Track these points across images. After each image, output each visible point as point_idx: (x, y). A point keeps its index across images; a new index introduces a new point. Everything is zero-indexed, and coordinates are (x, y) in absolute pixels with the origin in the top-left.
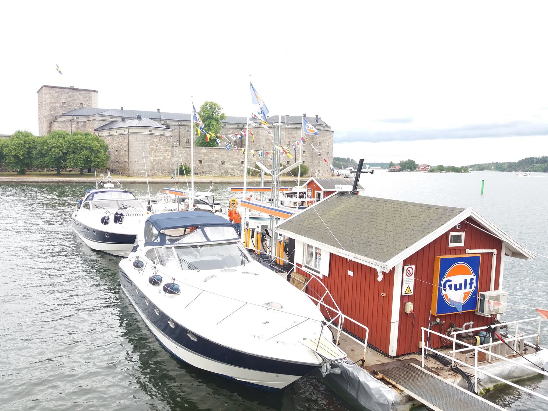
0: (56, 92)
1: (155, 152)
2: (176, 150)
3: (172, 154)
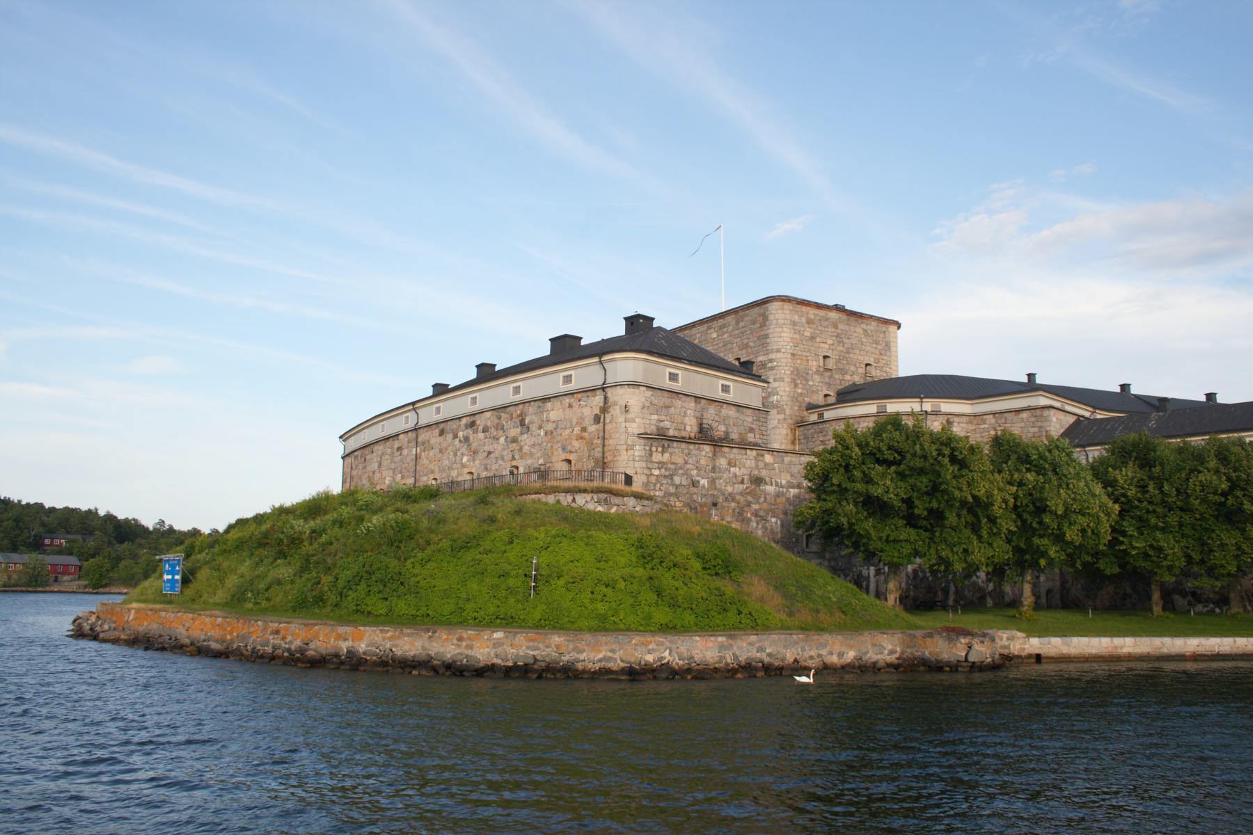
0: (809, 322)
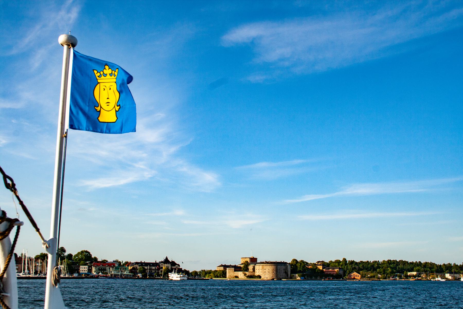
2: (235, 272)
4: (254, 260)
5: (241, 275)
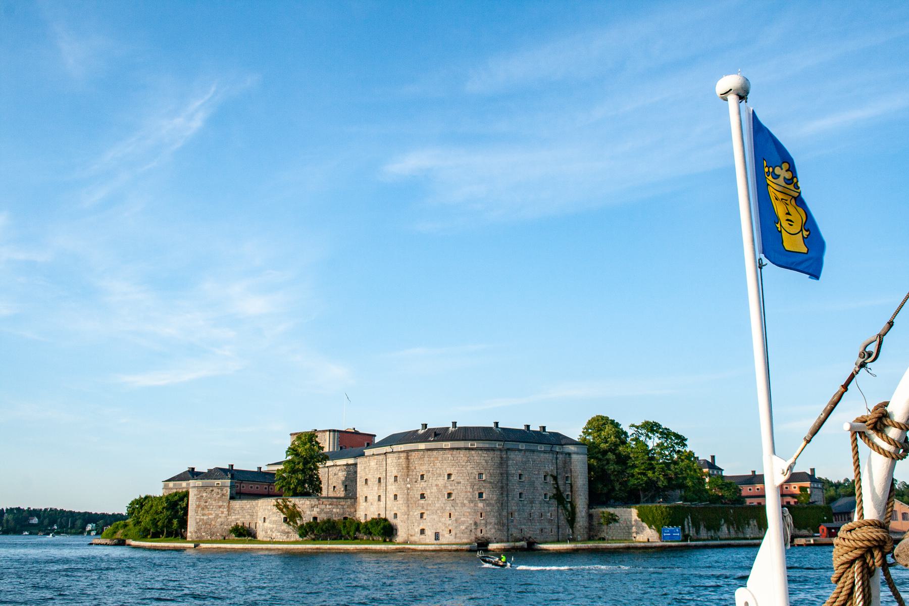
1: (203, 509)
2: (237, 504)
3: (228, 511)
4: (353, 443)
5: (265, 515)
